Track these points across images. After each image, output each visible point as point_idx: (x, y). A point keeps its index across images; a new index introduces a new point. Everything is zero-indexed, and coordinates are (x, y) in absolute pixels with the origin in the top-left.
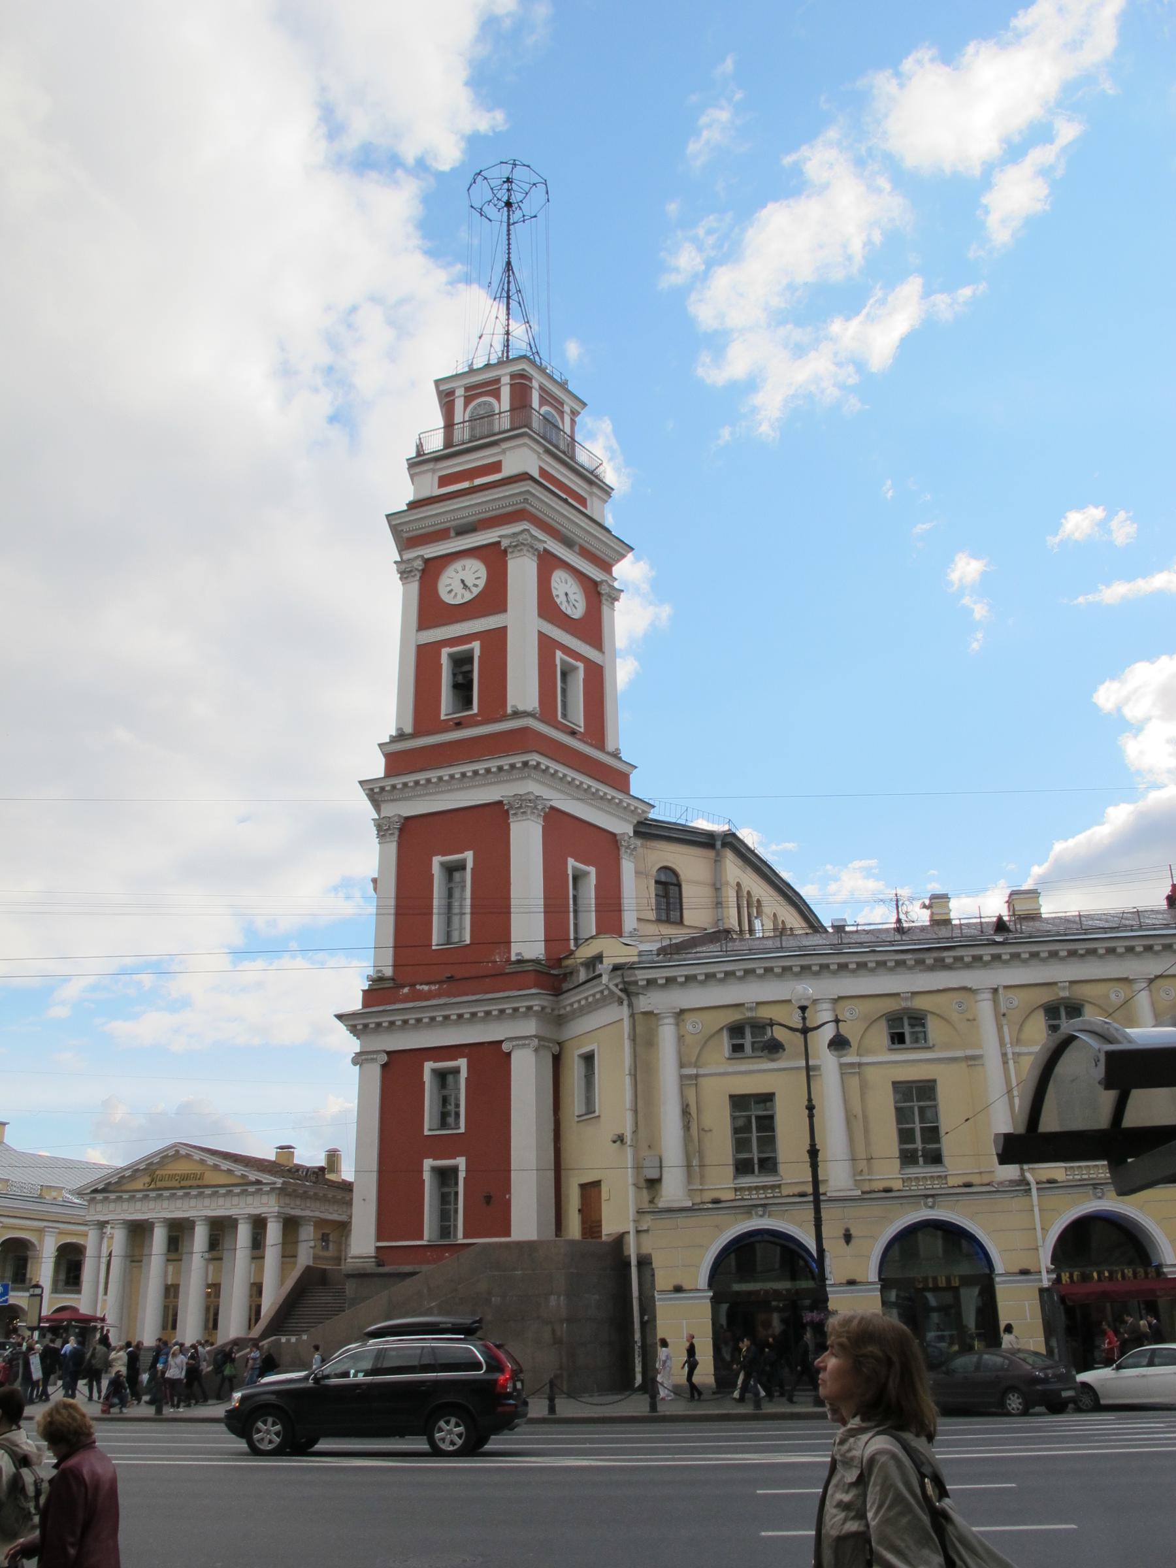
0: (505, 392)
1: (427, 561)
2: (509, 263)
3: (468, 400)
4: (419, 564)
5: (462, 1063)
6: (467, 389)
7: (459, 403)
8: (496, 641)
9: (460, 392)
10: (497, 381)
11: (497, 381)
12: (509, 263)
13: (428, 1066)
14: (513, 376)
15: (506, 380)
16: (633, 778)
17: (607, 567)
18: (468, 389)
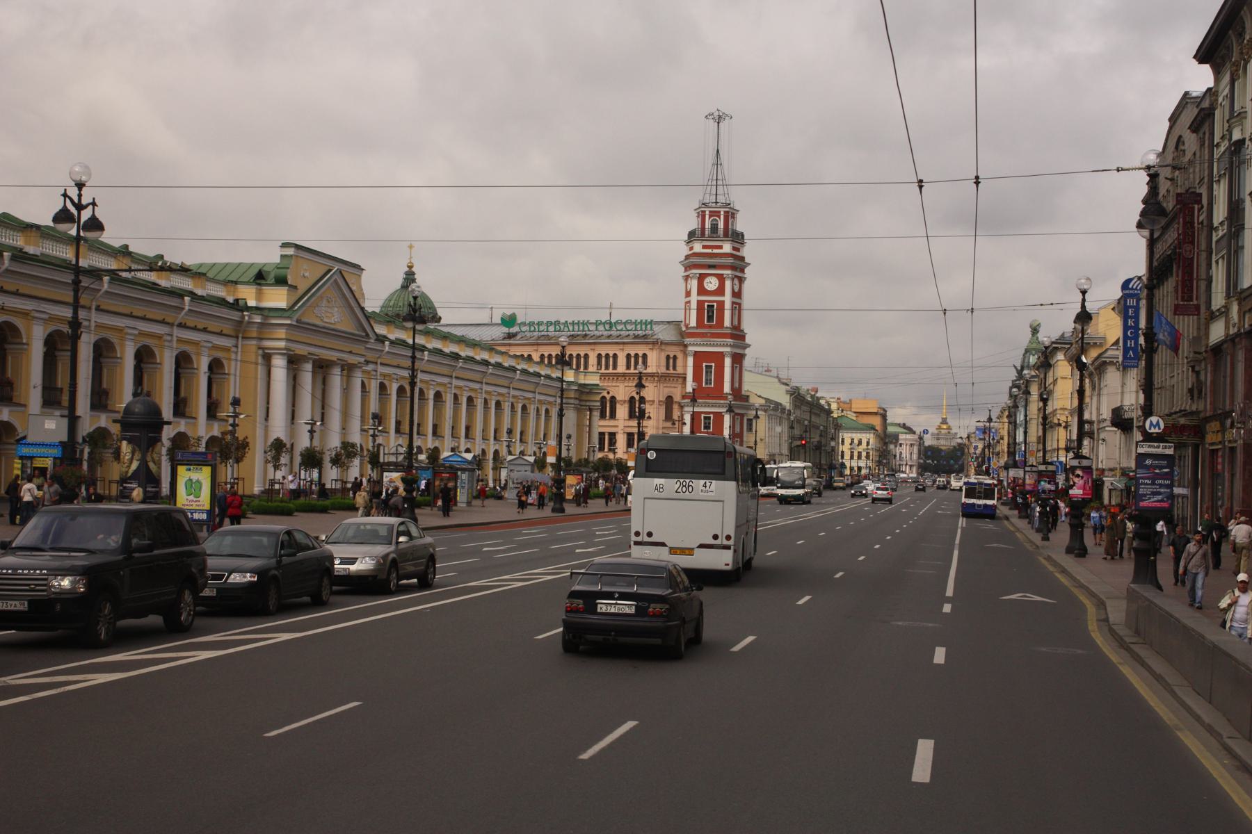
0: (722, 217)
1: (700, 274)
2: (718, 151)
3: (710, 217)
4: (698, 275)
5: (712, 416)
6: (710, 212)
7: (707, 217)
8: (721, 304)
9: (707, 213)
10: (720, 212)
11: (720, 212)
12: (718, 151)
13: (703, 416)
14: (725, 212)
15: (722, 213)
16: (747, 337)
17: (742, 271)
18: (710, 212)
